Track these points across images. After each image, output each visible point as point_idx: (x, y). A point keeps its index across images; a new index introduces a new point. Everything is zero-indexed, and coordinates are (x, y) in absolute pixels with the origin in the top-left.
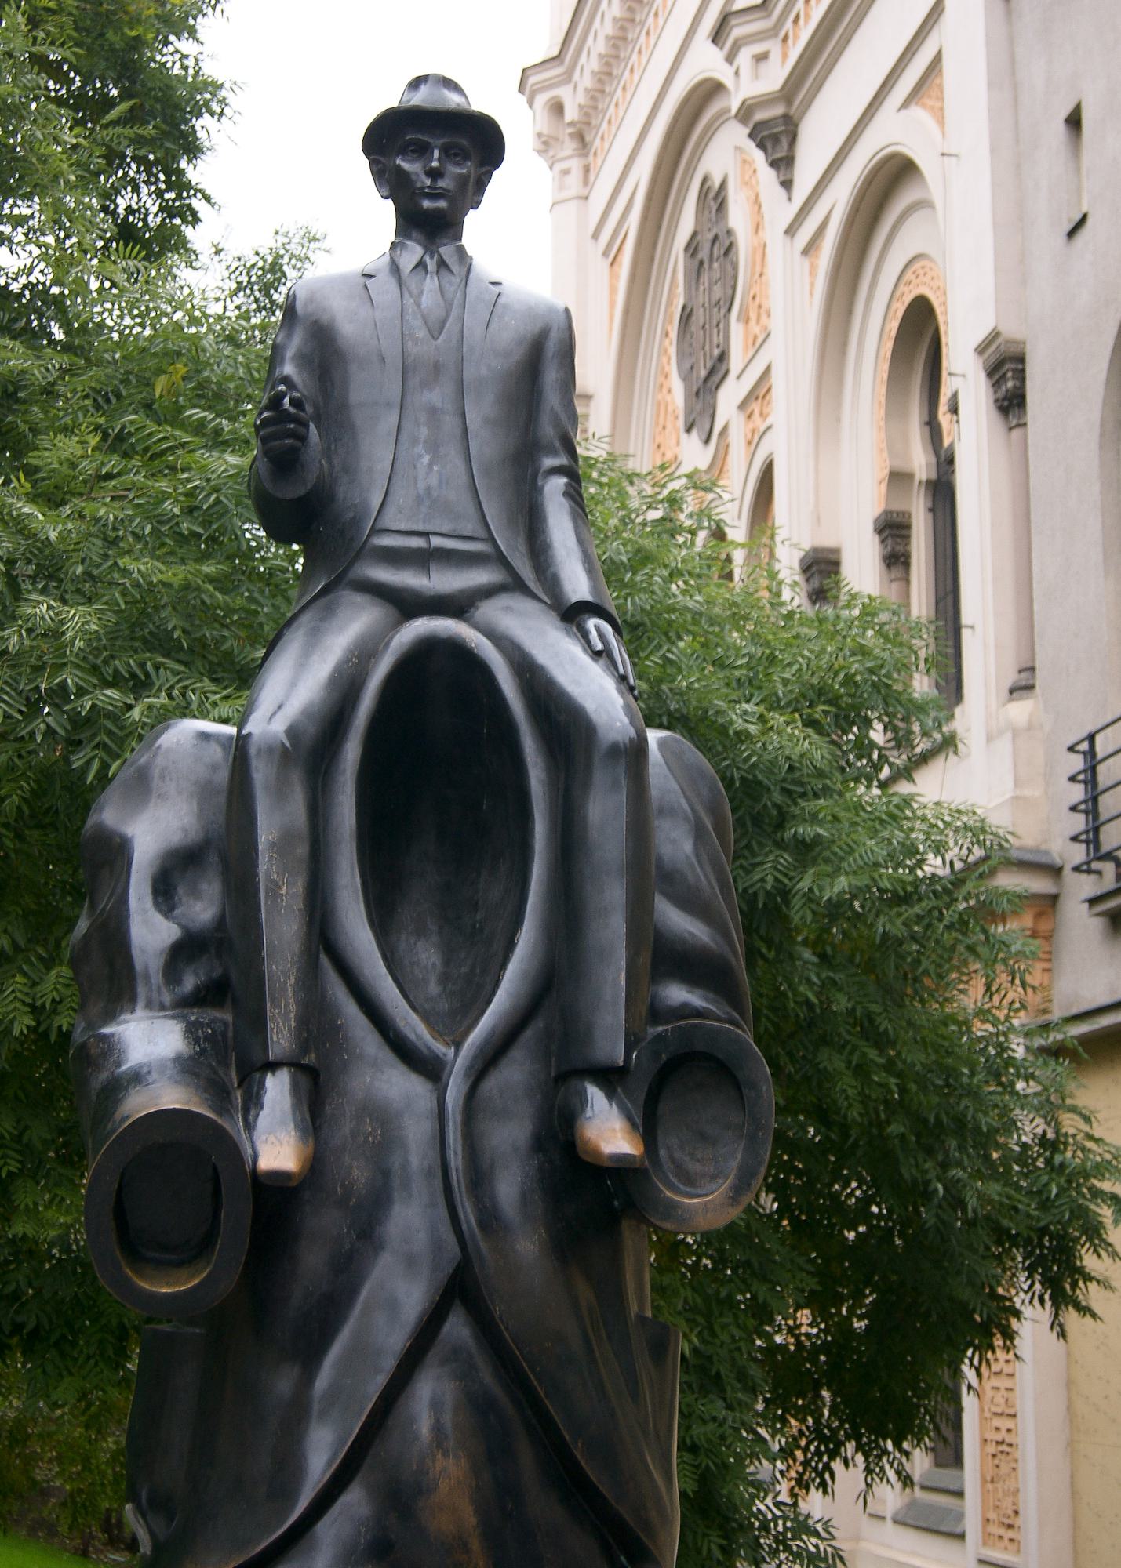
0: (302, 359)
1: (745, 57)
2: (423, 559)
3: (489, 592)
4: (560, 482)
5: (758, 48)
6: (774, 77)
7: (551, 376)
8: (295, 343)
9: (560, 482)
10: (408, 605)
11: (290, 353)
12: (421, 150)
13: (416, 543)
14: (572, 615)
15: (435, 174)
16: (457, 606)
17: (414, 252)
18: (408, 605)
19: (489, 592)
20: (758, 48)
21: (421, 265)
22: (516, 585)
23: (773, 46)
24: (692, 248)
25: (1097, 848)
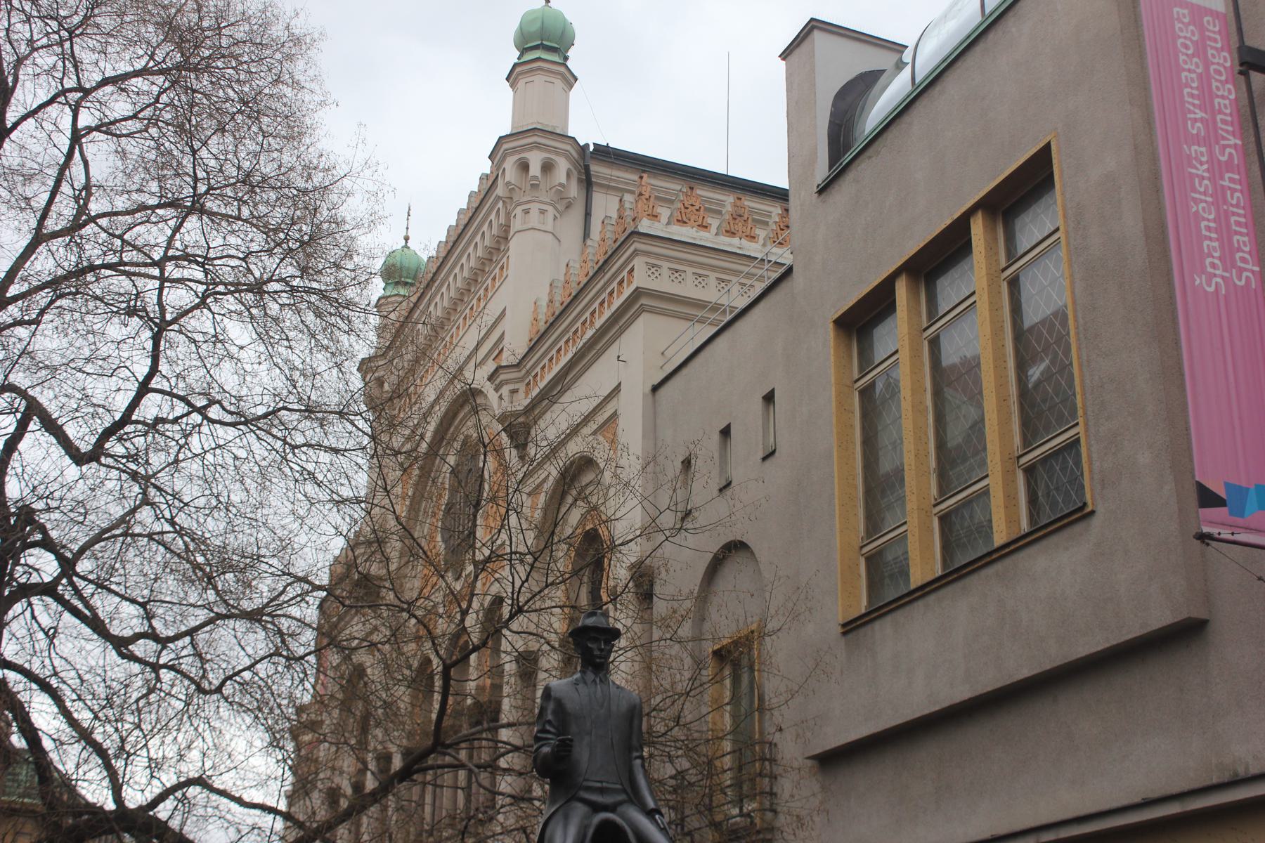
0: (554, 712)
1: (505, 390)
2: (602, 791)
3: (621, 803)
4: (638, 762)
5: (512, 387)
6: (522, 401)
7: (636, 722)
8: (551, 706)
9: (638, 762)
10: (596, 808)
11: (549, 712)
12: (596, 640)
13: (599, 785)
14: (650, 814)
15: (601, 650)
16: (612, 808)
17: (590, 676)
18: (596, 808)
19: (621, 803)
20: (512, 387)
21: (594, 681)
22: (630, 801)
23: (521, 387)
24: (454, 472)
25: (682, 829)
